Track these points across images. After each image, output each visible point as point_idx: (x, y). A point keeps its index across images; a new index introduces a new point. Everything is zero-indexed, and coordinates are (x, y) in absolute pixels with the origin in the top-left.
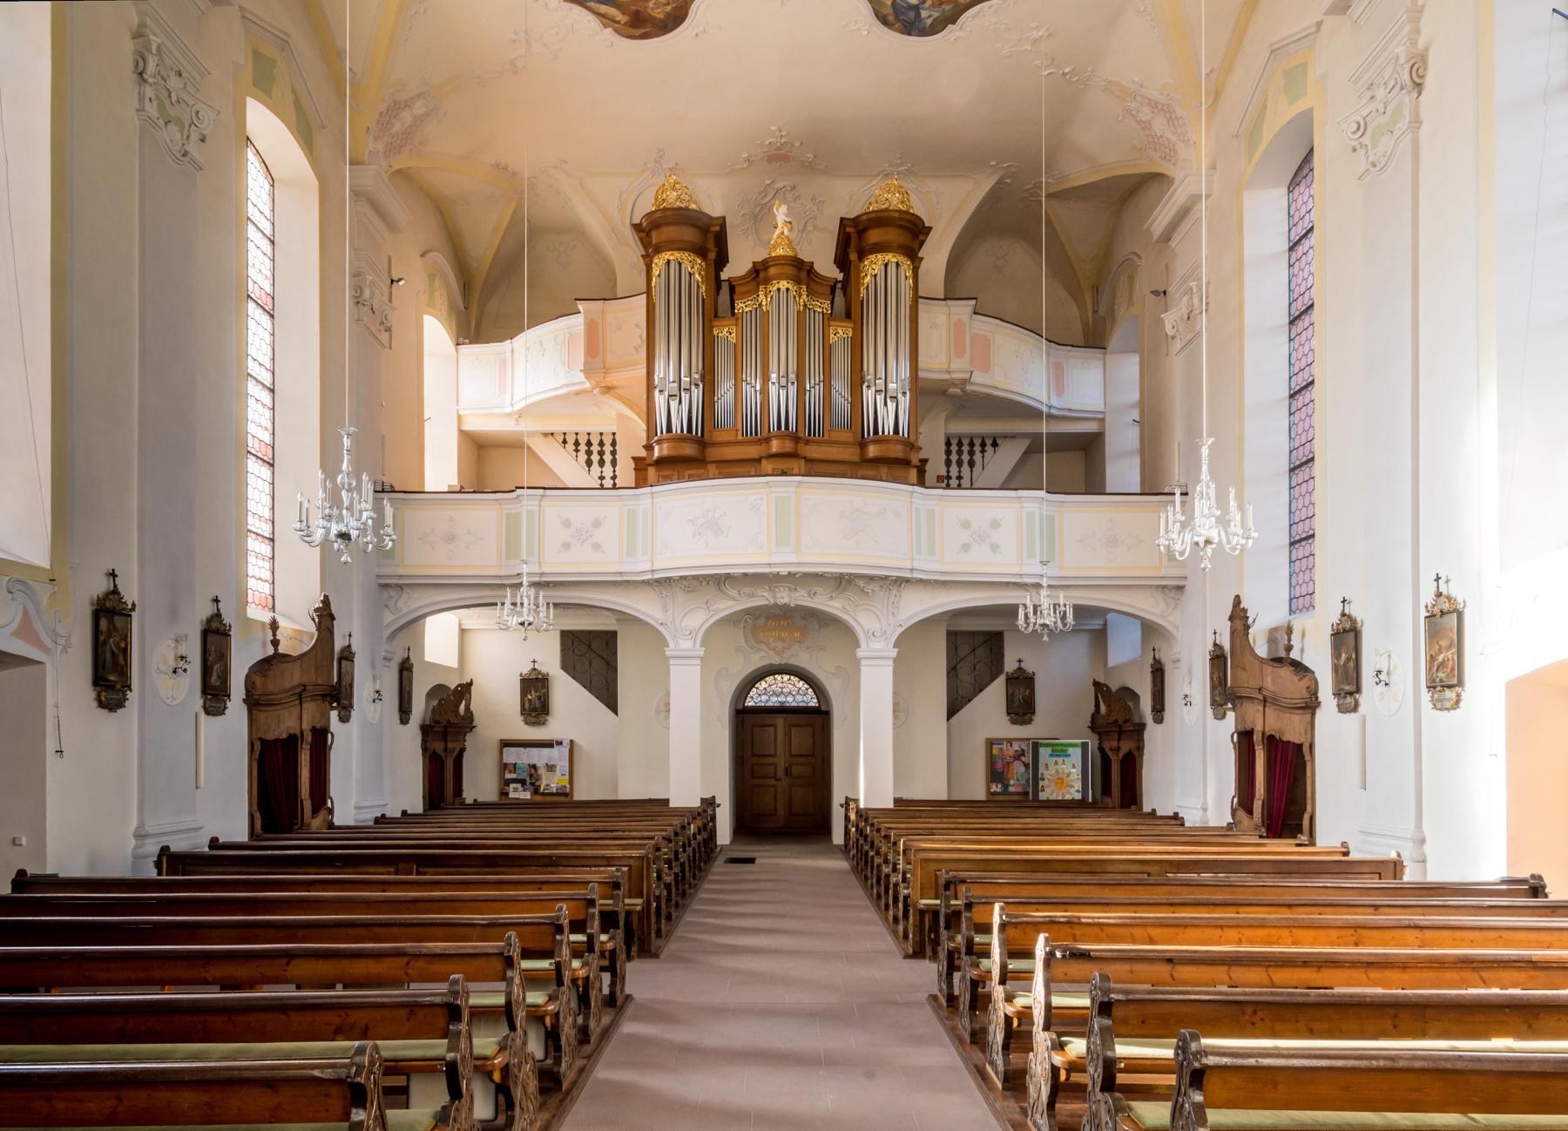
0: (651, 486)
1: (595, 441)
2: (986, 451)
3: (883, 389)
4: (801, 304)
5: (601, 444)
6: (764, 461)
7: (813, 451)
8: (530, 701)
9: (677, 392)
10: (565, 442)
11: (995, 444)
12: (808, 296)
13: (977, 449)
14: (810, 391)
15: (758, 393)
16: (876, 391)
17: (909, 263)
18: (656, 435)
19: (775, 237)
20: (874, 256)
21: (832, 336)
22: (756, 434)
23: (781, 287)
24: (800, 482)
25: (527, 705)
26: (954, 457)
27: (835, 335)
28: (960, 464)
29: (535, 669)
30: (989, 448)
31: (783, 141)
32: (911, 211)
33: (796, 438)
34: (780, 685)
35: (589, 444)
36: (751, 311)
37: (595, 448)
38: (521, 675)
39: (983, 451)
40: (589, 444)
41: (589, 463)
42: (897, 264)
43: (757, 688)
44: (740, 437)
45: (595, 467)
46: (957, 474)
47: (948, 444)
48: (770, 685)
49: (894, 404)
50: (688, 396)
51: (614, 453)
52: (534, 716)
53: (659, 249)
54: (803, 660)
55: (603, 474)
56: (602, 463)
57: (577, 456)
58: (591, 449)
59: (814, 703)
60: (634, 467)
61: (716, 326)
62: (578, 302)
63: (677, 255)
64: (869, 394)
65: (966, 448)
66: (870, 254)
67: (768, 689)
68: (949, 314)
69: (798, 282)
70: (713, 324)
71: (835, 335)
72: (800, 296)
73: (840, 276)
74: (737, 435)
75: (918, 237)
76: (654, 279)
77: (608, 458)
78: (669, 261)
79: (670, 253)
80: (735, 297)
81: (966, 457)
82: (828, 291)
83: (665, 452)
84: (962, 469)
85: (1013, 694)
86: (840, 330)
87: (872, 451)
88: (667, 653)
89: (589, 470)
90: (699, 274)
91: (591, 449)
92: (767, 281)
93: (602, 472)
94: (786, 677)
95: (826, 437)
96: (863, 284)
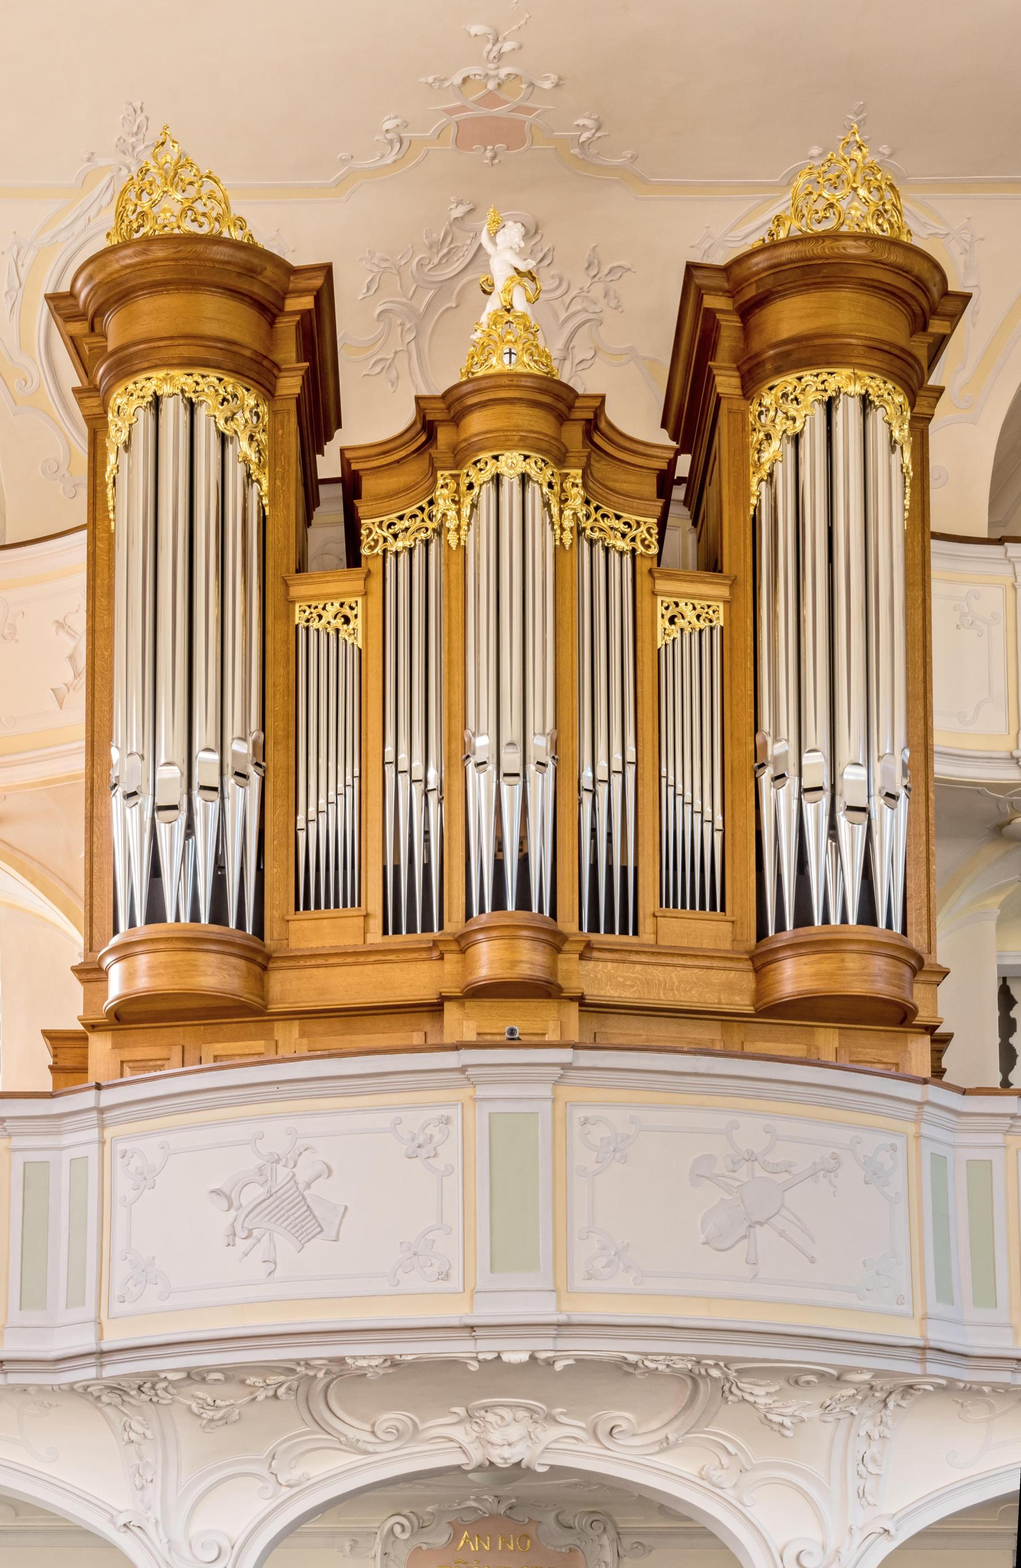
4: (568, 524)
12: (587, 502)
15: (433, 798)
16: (803, 791)
17: (900, 399)
19: (484, 319)
20: (791, 378)
21: (662, 624)
24: (565, 1067)
31: (503, 72)
32: (904, 238)
36: (411, 551)
42: (865, 402)
50: (214, 808)
61: (303, 598)
63: (181, 378)
66: (779, 371)
70: (295, 591)
71: (672, 621)
75: (925, 328)
79: (161, 374)
82: (649, 486)
90: (251, 438)
96: (759, 465)
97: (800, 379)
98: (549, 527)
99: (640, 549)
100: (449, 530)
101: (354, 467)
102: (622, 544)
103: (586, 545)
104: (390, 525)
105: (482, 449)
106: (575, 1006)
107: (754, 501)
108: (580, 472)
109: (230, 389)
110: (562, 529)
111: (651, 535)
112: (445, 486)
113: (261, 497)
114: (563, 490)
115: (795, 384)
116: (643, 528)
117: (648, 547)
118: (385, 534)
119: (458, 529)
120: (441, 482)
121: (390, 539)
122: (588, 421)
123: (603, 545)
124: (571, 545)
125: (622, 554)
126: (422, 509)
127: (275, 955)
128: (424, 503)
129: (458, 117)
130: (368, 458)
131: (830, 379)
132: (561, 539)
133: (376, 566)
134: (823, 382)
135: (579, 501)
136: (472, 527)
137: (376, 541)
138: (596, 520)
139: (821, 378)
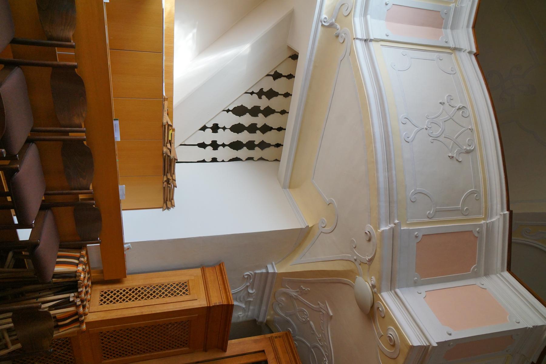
1: (272, 121)
35: (268, 112)
37: (260, 120)
40: (268, 112)
41: (239, 111)
45: (234, 120)
55: (220, 131)
58: (260, 115)
77: (244, 137)
89: (228, 111)
91: (260, 115)
93: (224, 128)
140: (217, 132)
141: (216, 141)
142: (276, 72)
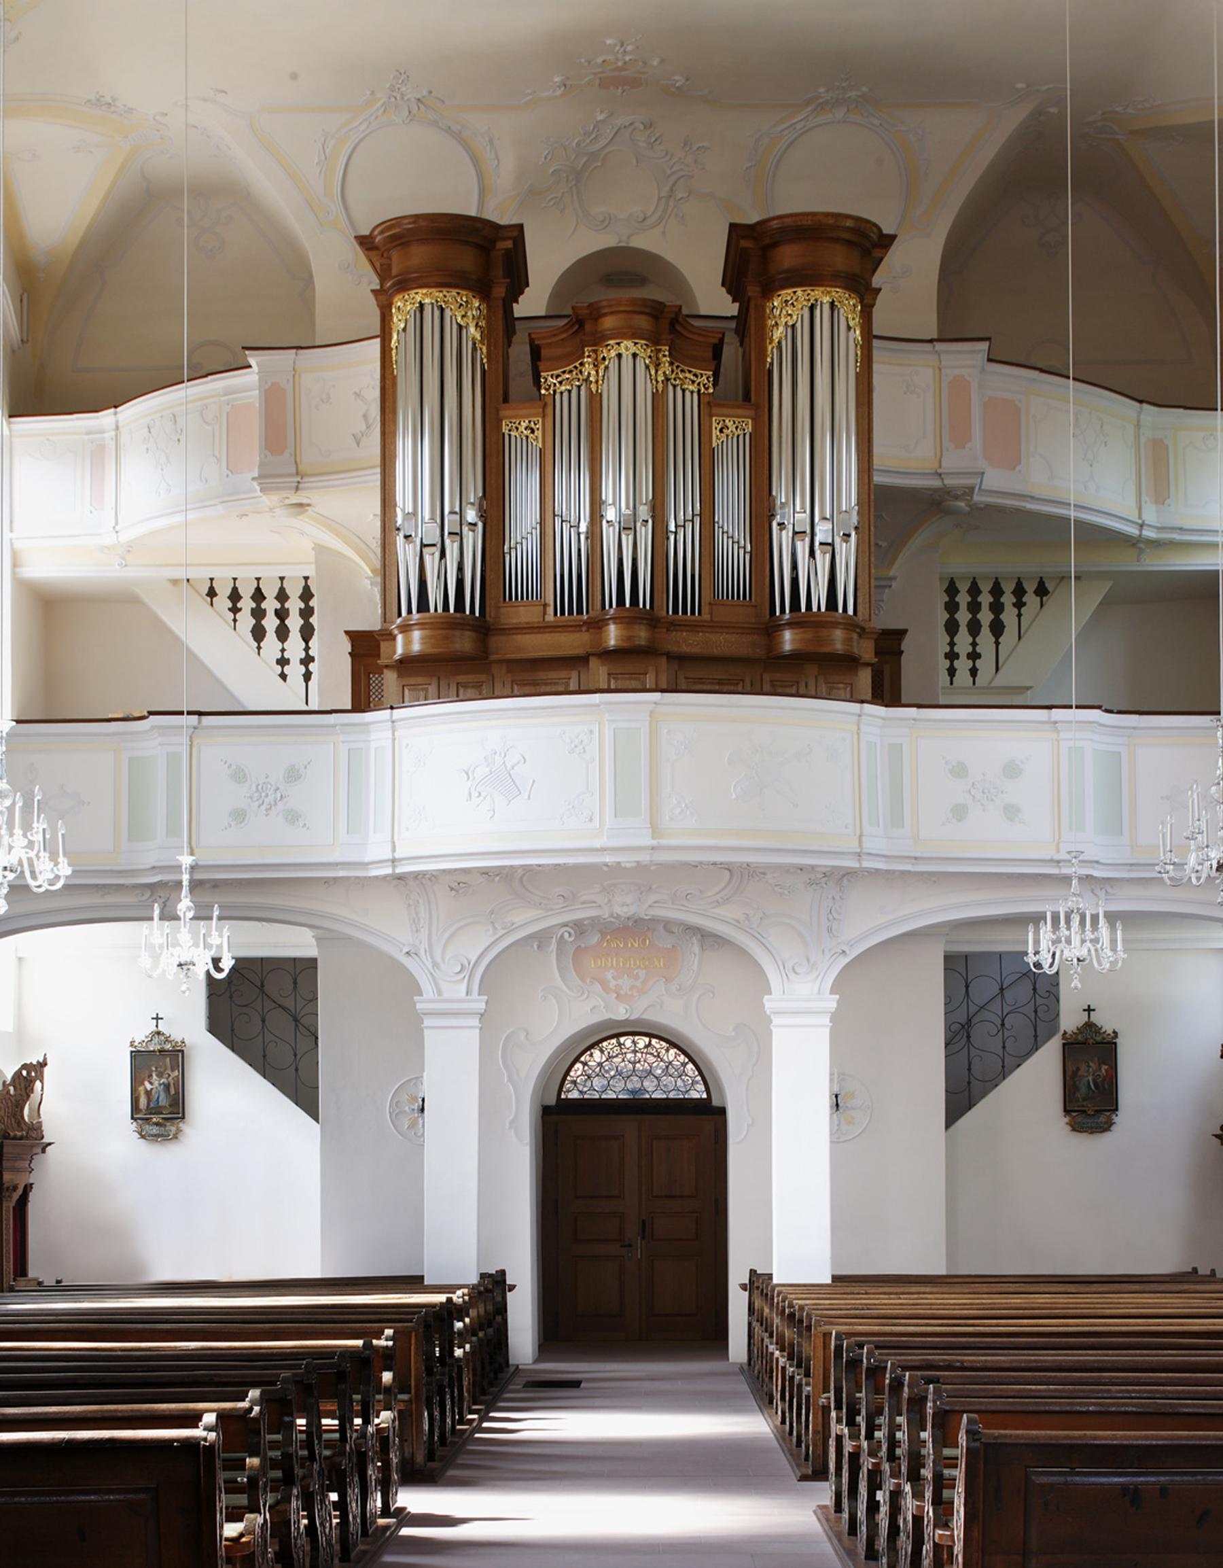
0: (392, 708)
1: (270, 592)
2: (1025, 604)
3: (808, 531)
4: (661, 378)
5: (282, 596)
6: (594, 662)
7: (688, 643)
8: (148, 1093)
9: (437, 540)
10: (212, 593)
11: (1042, 591)
12: (671, 364)
13: (1008, 599)
14: (676, 533)
15: (583, 537)
16: (795, 533)
18: (400, 615)
20: (789, 291)
21: (715, 433)
22: (580, 612)
23: (623, 351)
25: (143, 1102)
26: (963, 616)
27: (721, 431)
28: (974, 627)
29: (159, 1033)
30: (1031, 599)
31: (627, 58)
33: (651, 620)
34: (629, 1056)
35: (258, 596)
36: (570, 391)
37: (270, 605)
38: (132, 1044)
39: (1019, 605)
41: (258, 633)
42: (832, 304)
43: (585, 1064)
44: (550, 617)
46: (970, 649)
47: (952, 590)
48: (610, 1058)
49: (828, 556)
50: (456, 545)
51: (307, 613)
52: (157, 1124)
53: (403, 285)
54: (670, 1015)
55: (286, 655)
56: (282, 633)
57: (235, 620)
58: (263, 606)
59: (698, 1093)
60: (350, 651)
61: (506, 418)
62: (247, 352)
63: (437, 294)
64: (782, 540)
65: (985, 599)
66: (783, 288)
67: (607, 1065)
68: (940, 369)
69: (654, 340)
70: (502, 413)
71: (721, 431)
72: (657, 366)
73: (733, 309)
74: (545, 613)
76: (395, 337)
77: (294, 623)
78: (422, 305)
80: (542, 366)
81: (985, 617)
83: (416, 647)
84: (978, 640)
85: (1075, 1073)
86: (729, 423)
87: (788, 640)
88: (419, 1006)
89: (259, 648)
90: (477, 325)
91: (263, 606)
92: (598, 340)
93: (283, 650)
94: (642, 1042)
95: (706, 617)
96: (772, 341)
97: (795, 292)
98: (649, 381)
99: (703, 390)
100: (591, 382)
101: (537, 342)
102: (691, 387)
103: (671, 388)
104: (558, 376)
105: (611, 339)
106: (664, 660)
107: (769, 360)
108: (667, 348)
109: (464, 299)
110: (657, 382)
111: (709, 381)
112: (589, 356)
113: (482, 359)
114: (658, 358)
115: (792, 295)
116: (704, 377)
117: (707, 389)
118: (555, 381)
119: (597, 382)
120: (587, 354)
121: (557, 385)
122: (672, 319)
123: (681, 388)
124: (662, 391)
125: (692, 392)
126: (576, 367)
127: (492, 627)
128: (577, 364)
129: (599, 75)
130: (544, 338)
131: (812, 293)
132: (656, 388)
133: (550, 401)
134: (808, 295)
135: (667, 364)
136: (605, 381)
137: (550, 386)
138: (677, 373)
139: (806, 293)
140: (288, 660)
141: (301, 660)
142: (207, 595)
